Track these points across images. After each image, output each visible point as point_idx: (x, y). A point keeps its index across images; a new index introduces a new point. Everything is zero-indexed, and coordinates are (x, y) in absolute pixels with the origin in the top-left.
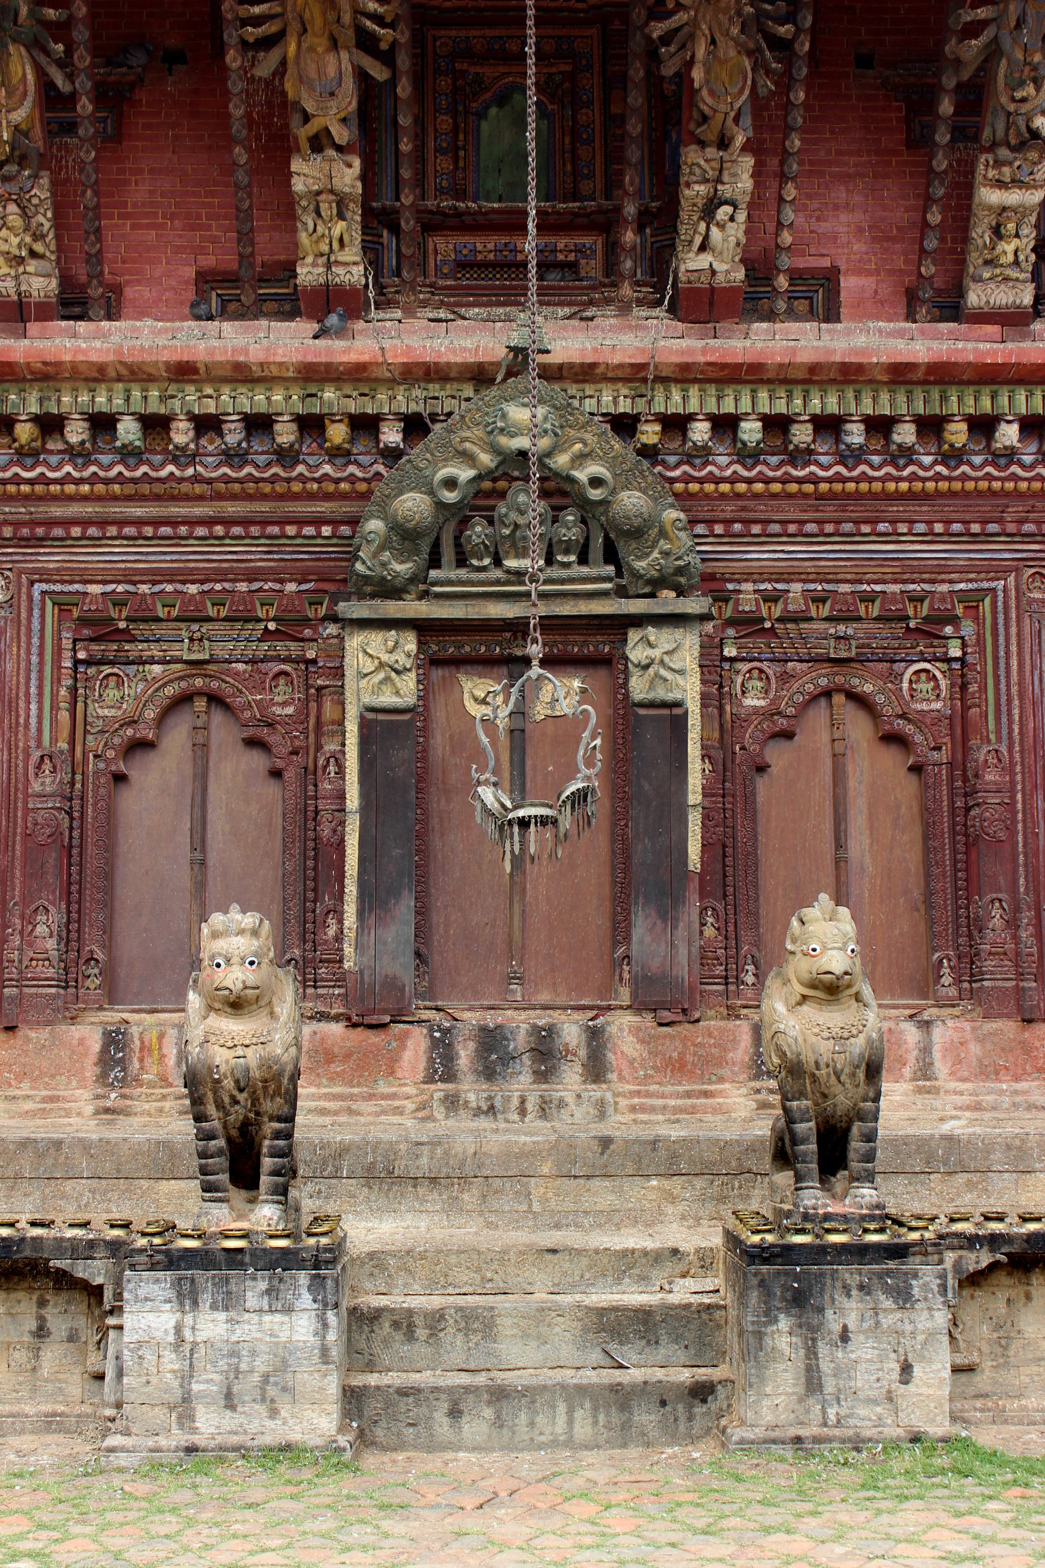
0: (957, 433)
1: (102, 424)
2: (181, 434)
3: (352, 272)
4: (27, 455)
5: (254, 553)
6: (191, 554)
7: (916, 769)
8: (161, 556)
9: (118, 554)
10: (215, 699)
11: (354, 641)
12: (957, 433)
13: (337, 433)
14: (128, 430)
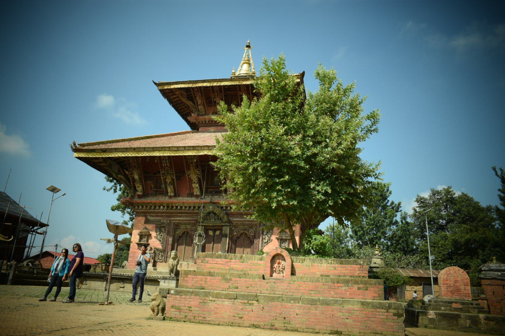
1: (177, 207)
2: (183, 208)
4: (171, 209)
5: (190, 219)
6: (185, 219)
14: (179, 207)
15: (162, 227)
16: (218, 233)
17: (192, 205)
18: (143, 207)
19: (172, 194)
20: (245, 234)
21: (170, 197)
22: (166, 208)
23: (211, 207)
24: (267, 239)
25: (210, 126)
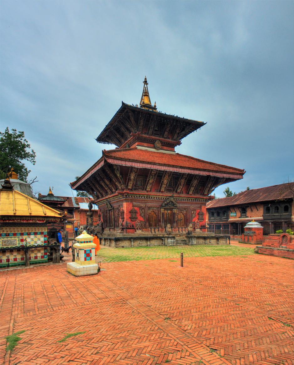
0: (188, 200)
1: (152, 197)
2: (155, 198)
3: (164, 190)
7: (184, 216)
8: (153, 204)
9: (151, 204)
10: (153, 211)
11: (161, 209)
12: (188, 200)
13: (162, 199)
14: (153, 198)
15: (142, 209)
16: (169, 211)
17: (160, 197)
18: (132, 196)
19: (149, 190)
20: (182, 212)
21: (148, 191)
22: (146, 198)
23: (172, 199)
24: (194, 215)
25: (144, 142)
